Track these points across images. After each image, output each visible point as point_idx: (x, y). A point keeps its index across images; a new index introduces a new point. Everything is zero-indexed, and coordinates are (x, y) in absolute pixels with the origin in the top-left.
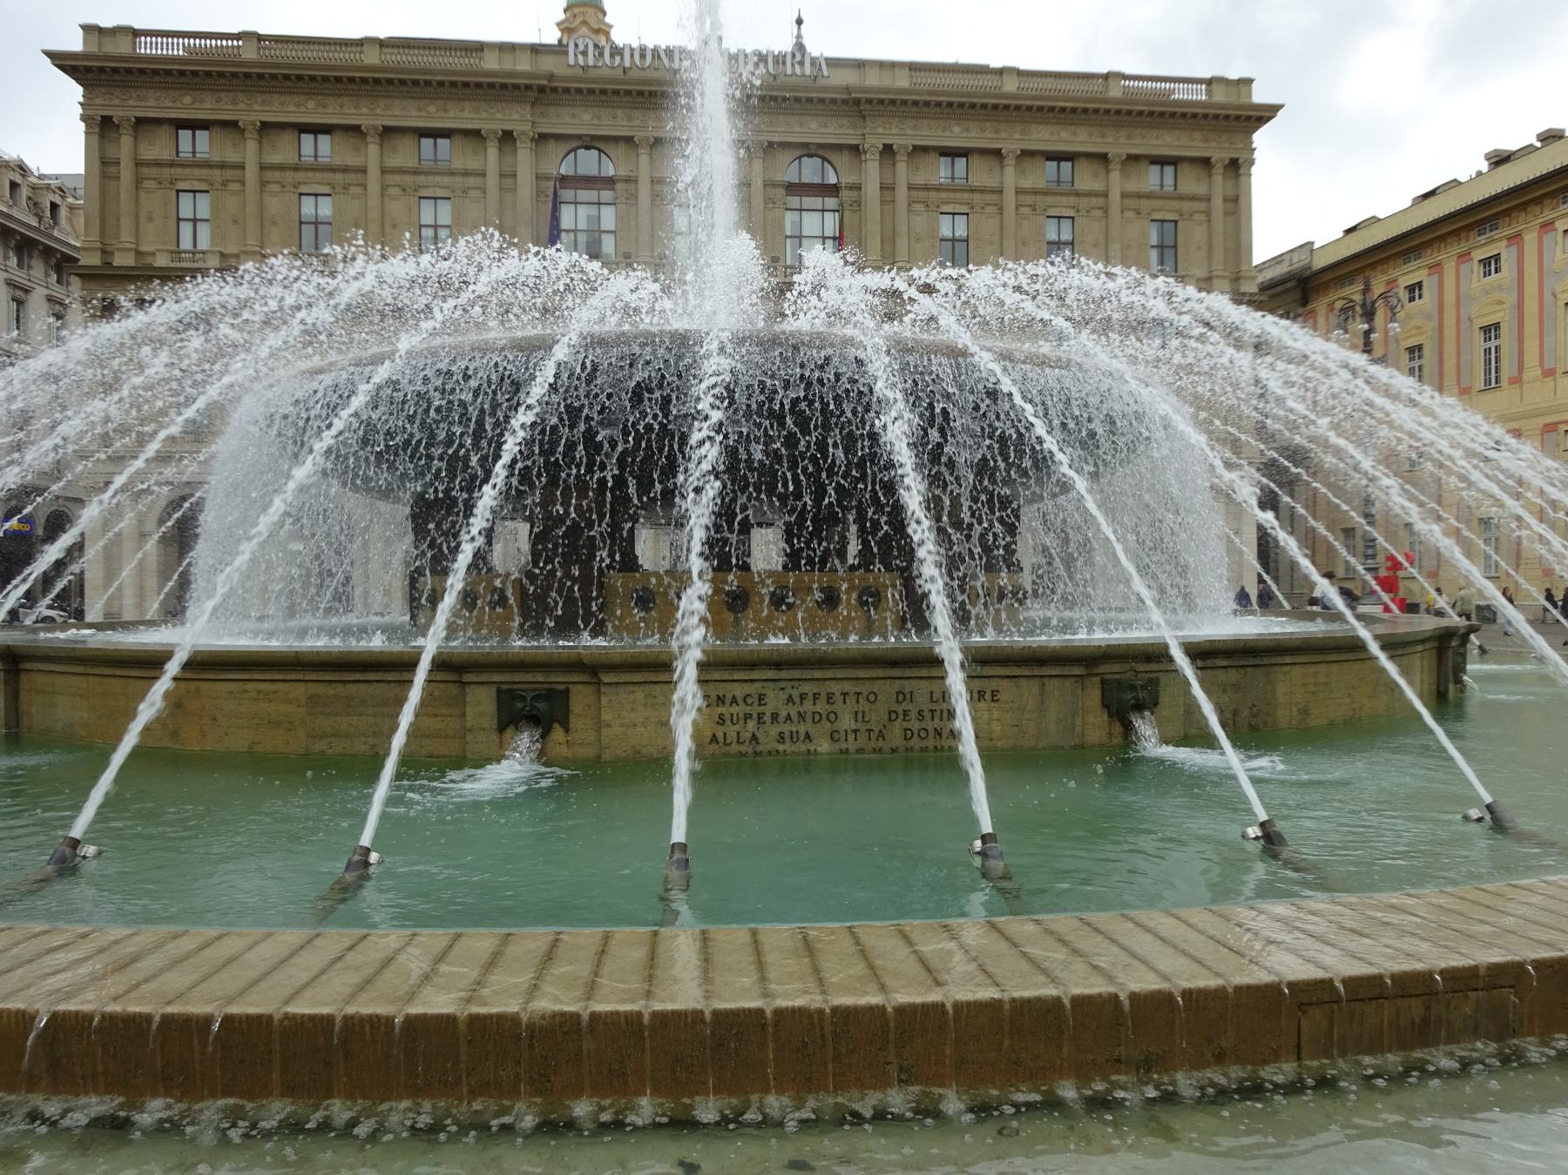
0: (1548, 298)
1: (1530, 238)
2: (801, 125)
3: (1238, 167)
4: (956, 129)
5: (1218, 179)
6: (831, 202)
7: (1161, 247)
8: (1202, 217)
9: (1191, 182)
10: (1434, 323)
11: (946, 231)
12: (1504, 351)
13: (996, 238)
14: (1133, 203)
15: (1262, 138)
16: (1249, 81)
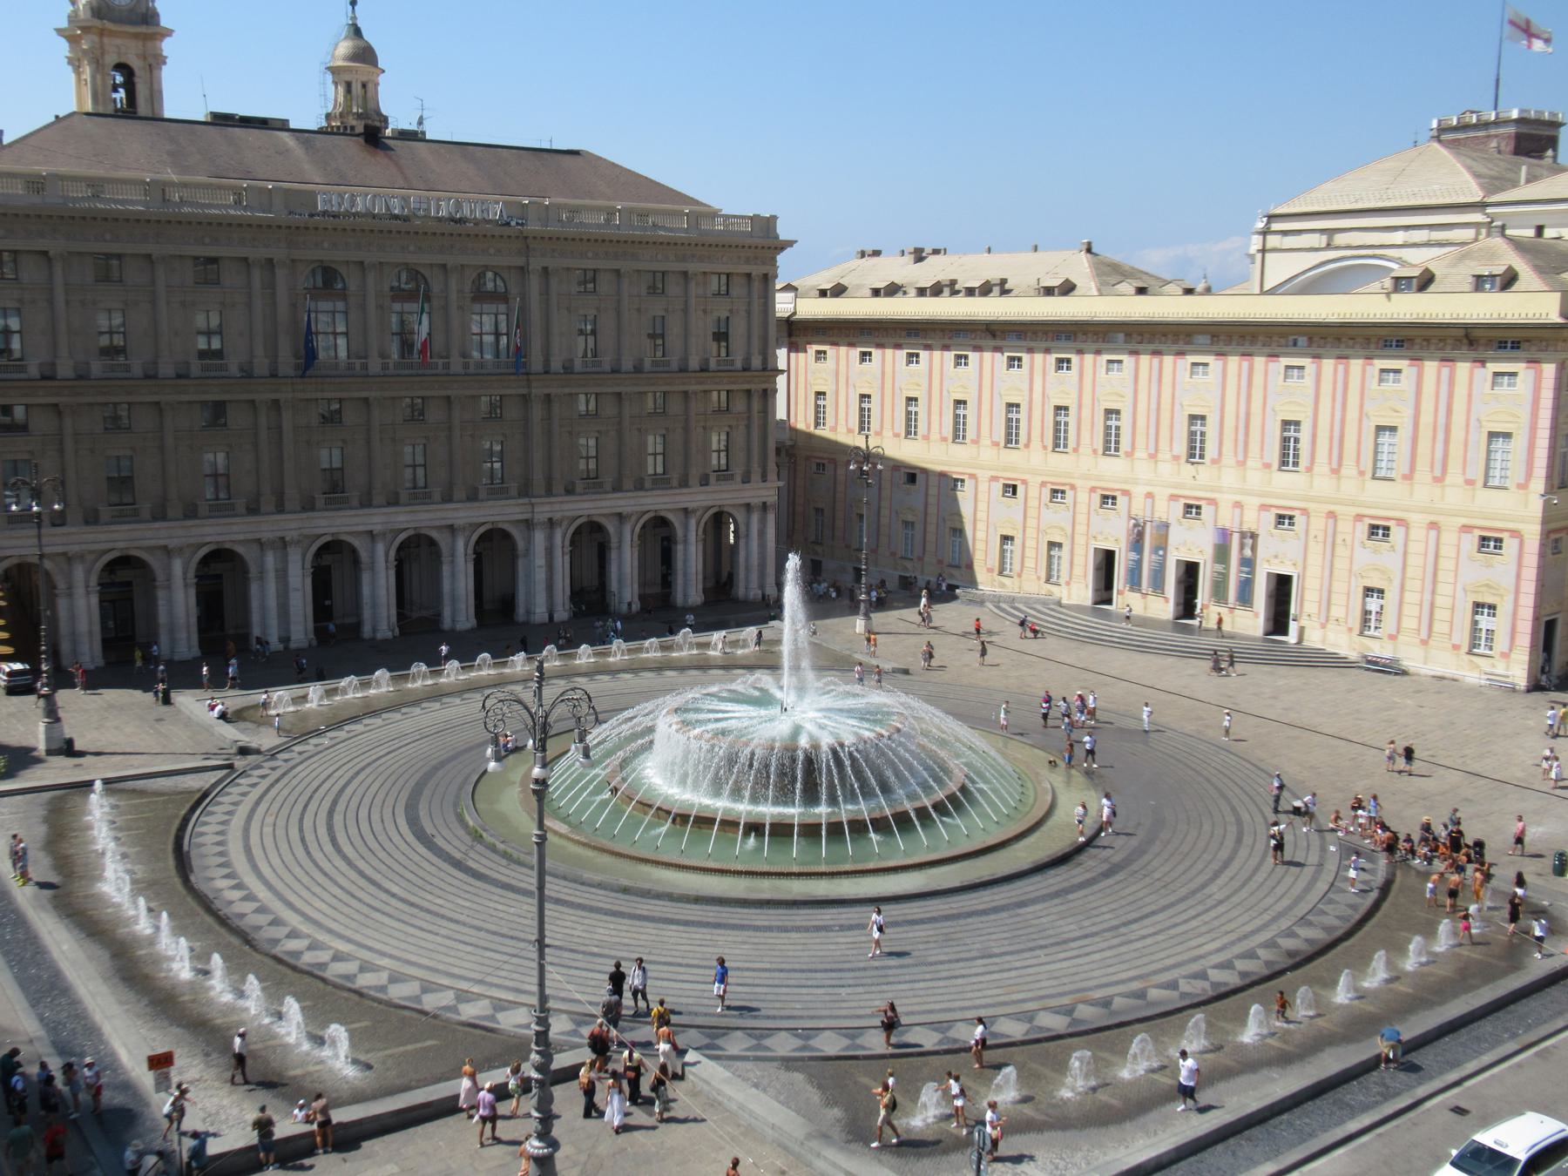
6: (502, 308)
15: (781, 259)
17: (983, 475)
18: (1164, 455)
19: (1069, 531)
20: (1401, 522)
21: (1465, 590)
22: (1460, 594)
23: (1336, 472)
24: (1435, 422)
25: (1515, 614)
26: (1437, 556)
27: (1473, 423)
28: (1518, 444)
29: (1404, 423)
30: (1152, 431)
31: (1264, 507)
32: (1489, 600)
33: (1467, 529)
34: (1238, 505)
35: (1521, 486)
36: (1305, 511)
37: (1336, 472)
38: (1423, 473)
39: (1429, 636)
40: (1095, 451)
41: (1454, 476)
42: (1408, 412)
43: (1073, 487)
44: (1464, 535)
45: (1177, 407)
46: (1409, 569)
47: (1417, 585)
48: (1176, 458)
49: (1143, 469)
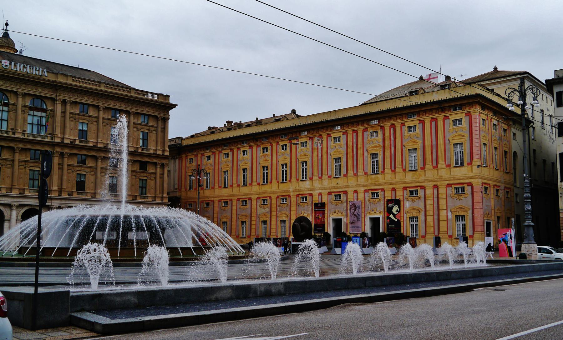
0: (239, 167)
1: (235, 150)
2: (36, 89)
3: (165, 120)
4: (86, 98)
5: (160, 122)
6: (44, 114)
7: (143, 139)
8: (154, 132)
9: (152, 123)
10: (213, 167)
11: (80, 128)
12: (229, 178)
13: (96, 132)
14: (136, 126)
15: (171, 112)
16: (169, 96)
17: (254, 197)
18: (325, 176)
19: (289, 215)
20: (423, 187)
21: (451, 211)
22: (450, 214)
23: (394, 171)
24: (432, 144)
25: (473, 217)
27: (447, 142)
29: (419, 146)
30: (320, 168)
31: (366, 191)
32: (462, 213)
33: (449, 185)
34: (356, 192)
35: (468, 164)
36: (383, 190)
37: (394, 171)
38: (429, 166)
40: (297, 180)
41: (442, 165)
42: (420, 142)
43: (289, 196)
45: (329, 156)
46: (427, 207)
47: (431, 213)
48: (330, 177)
49: (317, 184)
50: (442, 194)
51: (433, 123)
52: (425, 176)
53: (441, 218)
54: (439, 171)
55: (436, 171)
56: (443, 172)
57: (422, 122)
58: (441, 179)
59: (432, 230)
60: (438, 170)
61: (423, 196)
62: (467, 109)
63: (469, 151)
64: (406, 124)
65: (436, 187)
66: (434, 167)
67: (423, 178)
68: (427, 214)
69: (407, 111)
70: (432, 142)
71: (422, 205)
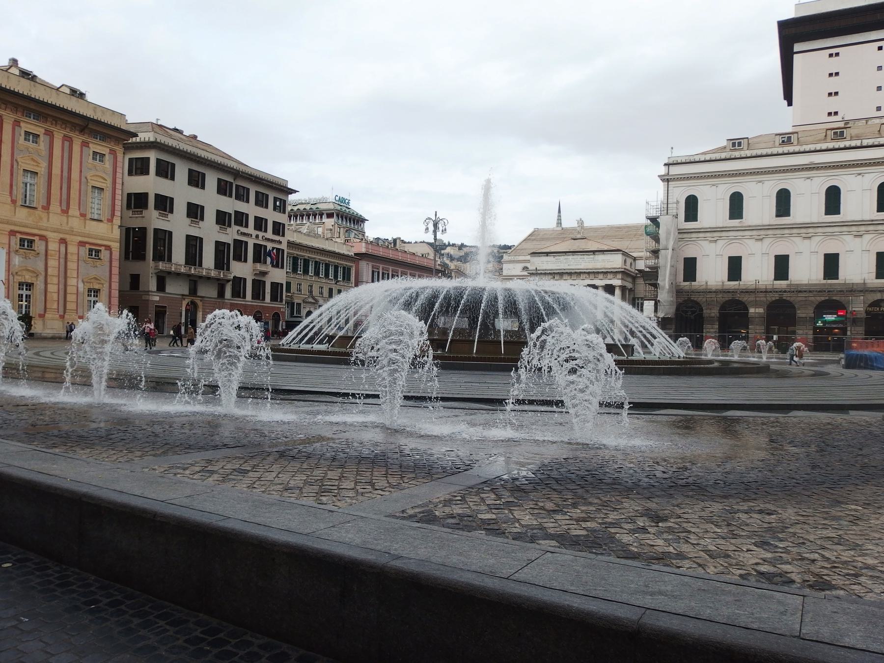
20: (43, 238)
21: (83, 281)
22: (81, 285)
24: (62, 175)
25: (110, 292)
26: (66, 258)
27: (83, 179)
28: (108, 194)
29: (42, 169)
32: (97, 287)
33: (82, 244)
38: (55, 207)
39: (65, 312)
41: (74, 211)
42: (44, 164)
44: (81, 248)
46: (49, 270)
47: (55, 280)
50: (72, 254)
51: (67, 144)
52: (48, 220)
53: (69, 289)
54: (70, 219)
55: (64, 219)
56: (75, 223)
57: (49, 133)
58: (71, 232)
59: (55, 306)
60: (68, 217)
61: (43, 252)
62: (112, 144)
63: (110, 203)
64: (22, 124)
65: (63, 241)
66: (62, 211)
67: (44, 224)
68: (49, 281)
69: (32, 106)
70: (62, 172)
71: (40, 266)
